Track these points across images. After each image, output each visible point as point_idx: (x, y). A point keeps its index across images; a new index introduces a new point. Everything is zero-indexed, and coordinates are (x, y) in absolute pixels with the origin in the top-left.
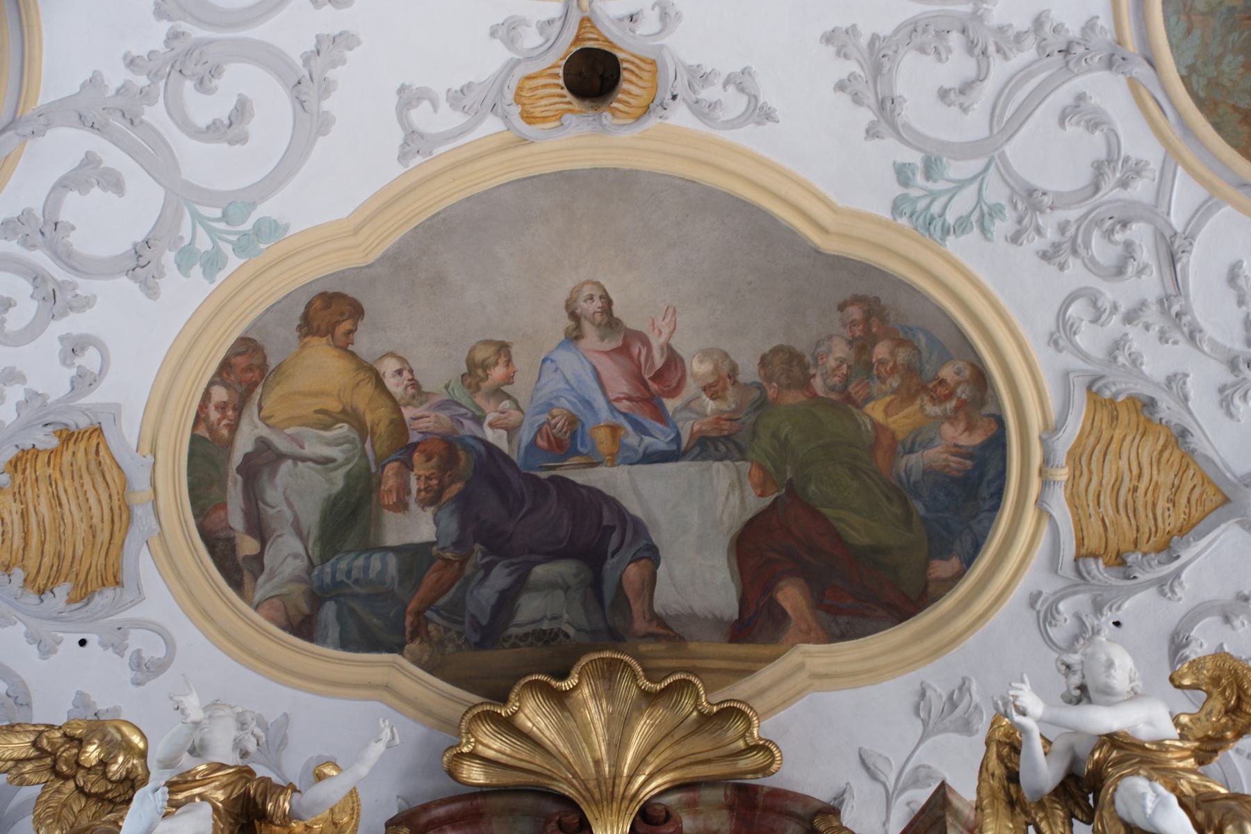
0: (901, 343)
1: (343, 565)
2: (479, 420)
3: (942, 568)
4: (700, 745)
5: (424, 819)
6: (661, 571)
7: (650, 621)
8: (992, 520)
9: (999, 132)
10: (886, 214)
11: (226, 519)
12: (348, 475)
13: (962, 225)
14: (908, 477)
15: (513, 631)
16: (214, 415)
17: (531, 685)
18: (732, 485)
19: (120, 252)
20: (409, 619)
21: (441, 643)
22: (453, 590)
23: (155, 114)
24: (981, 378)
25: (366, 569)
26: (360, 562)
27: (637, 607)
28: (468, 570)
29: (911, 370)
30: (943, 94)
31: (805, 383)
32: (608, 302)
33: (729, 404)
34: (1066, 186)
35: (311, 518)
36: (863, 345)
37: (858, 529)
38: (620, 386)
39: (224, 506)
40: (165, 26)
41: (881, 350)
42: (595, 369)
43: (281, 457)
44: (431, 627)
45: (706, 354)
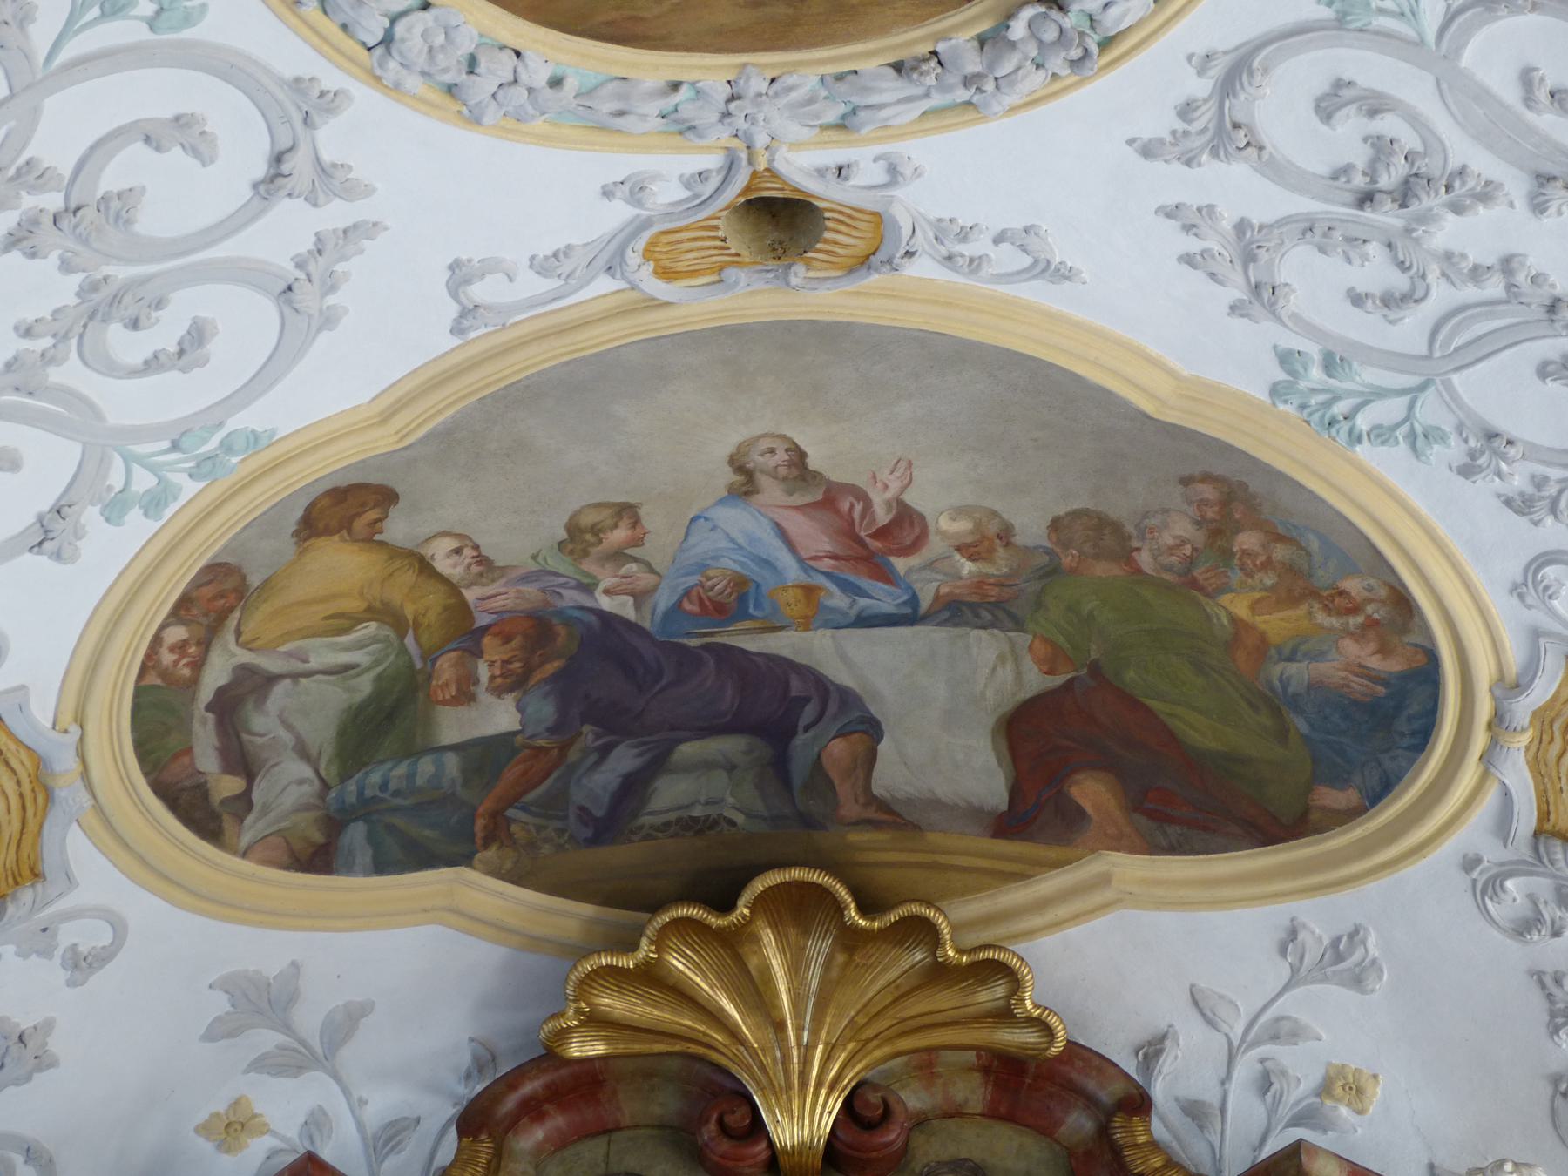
0: (1280, 538)
1: (375, 777)
2: (588, 588)
3: (1332, 798)
4: (944, 1000)
5: (510, 1103)
6: (884, 747)
7: (867, 805)
8: (1412, 761)
9: (1443, 357)
10: (1263, 396)
11: (192, 763)
12: (379, 678)
13: (1382, 434)
14: (1285, 688)
15: (646, 820)
16: (167, 658)
17: (676, 922)
18: (1001, 658)
19: (20, 529)
20: (480, 823)
21: (532, 845)
22: (550, 781)
23: (70, 373)
24: (1402, 602)
25: (411, 776)
26: (402, 769)
27: (844, 790)
28: (573, 755)
29: (1291, 570)
30: (1357, 299)
31: (1126, 555)
32: (798, 457)
33: (1000, 565)
34: (1545, 439)
35: (322, 731)
36: (1219, 531)
37: (1200, 731)
38: (815, 537)
39: (188, 751)
40: (76, 279)
41: (1248, 540)
42: (777, 524)
43: (272, 679)
44: (514, 828)
45: (959, 512)
